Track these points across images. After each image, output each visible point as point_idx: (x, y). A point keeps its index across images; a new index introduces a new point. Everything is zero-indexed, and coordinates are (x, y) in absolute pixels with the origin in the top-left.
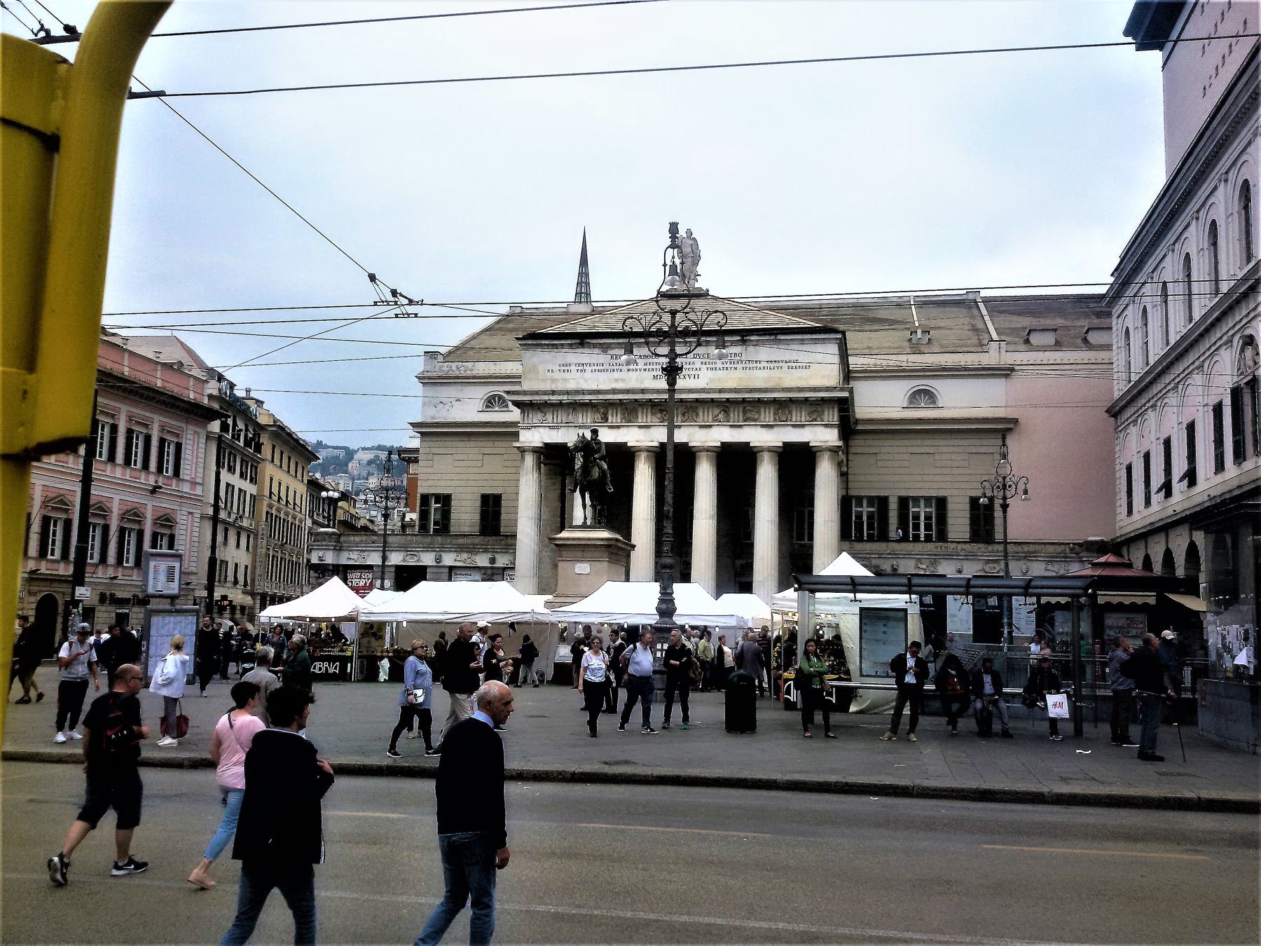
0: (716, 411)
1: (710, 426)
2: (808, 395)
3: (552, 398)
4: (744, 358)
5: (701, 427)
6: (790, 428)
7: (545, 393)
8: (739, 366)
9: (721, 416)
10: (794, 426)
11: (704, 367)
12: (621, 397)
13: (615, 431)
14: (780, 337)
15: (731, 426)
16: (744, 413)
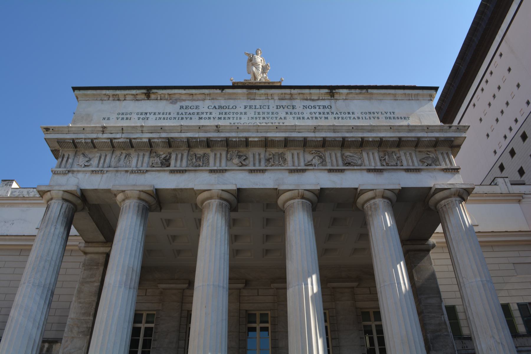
0: (309, 157)
1: (303, 171)
2: (420, 135)
3: (100, 135)
4: (333, 110)
5: (291, 171)
6: (403, 174)
7: (93, 130)
8: (330, 116)
9: (316, 161)
10: (407, 170)
11: (288, 116)
12: (189, 135)
13: (178, 176)
14: (370, 91)
15: (330, 171)
16: (343, 160)
